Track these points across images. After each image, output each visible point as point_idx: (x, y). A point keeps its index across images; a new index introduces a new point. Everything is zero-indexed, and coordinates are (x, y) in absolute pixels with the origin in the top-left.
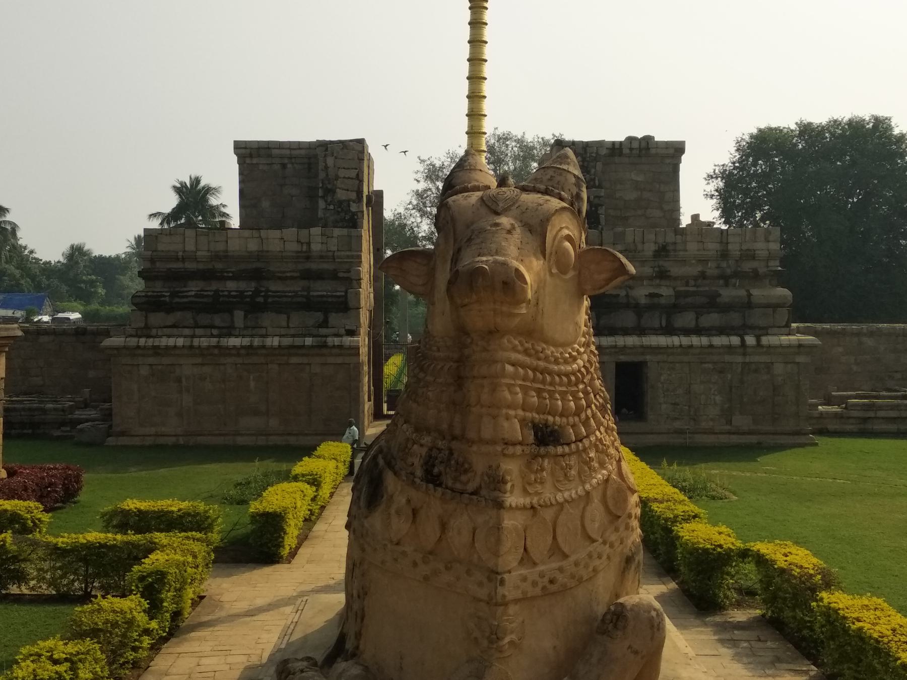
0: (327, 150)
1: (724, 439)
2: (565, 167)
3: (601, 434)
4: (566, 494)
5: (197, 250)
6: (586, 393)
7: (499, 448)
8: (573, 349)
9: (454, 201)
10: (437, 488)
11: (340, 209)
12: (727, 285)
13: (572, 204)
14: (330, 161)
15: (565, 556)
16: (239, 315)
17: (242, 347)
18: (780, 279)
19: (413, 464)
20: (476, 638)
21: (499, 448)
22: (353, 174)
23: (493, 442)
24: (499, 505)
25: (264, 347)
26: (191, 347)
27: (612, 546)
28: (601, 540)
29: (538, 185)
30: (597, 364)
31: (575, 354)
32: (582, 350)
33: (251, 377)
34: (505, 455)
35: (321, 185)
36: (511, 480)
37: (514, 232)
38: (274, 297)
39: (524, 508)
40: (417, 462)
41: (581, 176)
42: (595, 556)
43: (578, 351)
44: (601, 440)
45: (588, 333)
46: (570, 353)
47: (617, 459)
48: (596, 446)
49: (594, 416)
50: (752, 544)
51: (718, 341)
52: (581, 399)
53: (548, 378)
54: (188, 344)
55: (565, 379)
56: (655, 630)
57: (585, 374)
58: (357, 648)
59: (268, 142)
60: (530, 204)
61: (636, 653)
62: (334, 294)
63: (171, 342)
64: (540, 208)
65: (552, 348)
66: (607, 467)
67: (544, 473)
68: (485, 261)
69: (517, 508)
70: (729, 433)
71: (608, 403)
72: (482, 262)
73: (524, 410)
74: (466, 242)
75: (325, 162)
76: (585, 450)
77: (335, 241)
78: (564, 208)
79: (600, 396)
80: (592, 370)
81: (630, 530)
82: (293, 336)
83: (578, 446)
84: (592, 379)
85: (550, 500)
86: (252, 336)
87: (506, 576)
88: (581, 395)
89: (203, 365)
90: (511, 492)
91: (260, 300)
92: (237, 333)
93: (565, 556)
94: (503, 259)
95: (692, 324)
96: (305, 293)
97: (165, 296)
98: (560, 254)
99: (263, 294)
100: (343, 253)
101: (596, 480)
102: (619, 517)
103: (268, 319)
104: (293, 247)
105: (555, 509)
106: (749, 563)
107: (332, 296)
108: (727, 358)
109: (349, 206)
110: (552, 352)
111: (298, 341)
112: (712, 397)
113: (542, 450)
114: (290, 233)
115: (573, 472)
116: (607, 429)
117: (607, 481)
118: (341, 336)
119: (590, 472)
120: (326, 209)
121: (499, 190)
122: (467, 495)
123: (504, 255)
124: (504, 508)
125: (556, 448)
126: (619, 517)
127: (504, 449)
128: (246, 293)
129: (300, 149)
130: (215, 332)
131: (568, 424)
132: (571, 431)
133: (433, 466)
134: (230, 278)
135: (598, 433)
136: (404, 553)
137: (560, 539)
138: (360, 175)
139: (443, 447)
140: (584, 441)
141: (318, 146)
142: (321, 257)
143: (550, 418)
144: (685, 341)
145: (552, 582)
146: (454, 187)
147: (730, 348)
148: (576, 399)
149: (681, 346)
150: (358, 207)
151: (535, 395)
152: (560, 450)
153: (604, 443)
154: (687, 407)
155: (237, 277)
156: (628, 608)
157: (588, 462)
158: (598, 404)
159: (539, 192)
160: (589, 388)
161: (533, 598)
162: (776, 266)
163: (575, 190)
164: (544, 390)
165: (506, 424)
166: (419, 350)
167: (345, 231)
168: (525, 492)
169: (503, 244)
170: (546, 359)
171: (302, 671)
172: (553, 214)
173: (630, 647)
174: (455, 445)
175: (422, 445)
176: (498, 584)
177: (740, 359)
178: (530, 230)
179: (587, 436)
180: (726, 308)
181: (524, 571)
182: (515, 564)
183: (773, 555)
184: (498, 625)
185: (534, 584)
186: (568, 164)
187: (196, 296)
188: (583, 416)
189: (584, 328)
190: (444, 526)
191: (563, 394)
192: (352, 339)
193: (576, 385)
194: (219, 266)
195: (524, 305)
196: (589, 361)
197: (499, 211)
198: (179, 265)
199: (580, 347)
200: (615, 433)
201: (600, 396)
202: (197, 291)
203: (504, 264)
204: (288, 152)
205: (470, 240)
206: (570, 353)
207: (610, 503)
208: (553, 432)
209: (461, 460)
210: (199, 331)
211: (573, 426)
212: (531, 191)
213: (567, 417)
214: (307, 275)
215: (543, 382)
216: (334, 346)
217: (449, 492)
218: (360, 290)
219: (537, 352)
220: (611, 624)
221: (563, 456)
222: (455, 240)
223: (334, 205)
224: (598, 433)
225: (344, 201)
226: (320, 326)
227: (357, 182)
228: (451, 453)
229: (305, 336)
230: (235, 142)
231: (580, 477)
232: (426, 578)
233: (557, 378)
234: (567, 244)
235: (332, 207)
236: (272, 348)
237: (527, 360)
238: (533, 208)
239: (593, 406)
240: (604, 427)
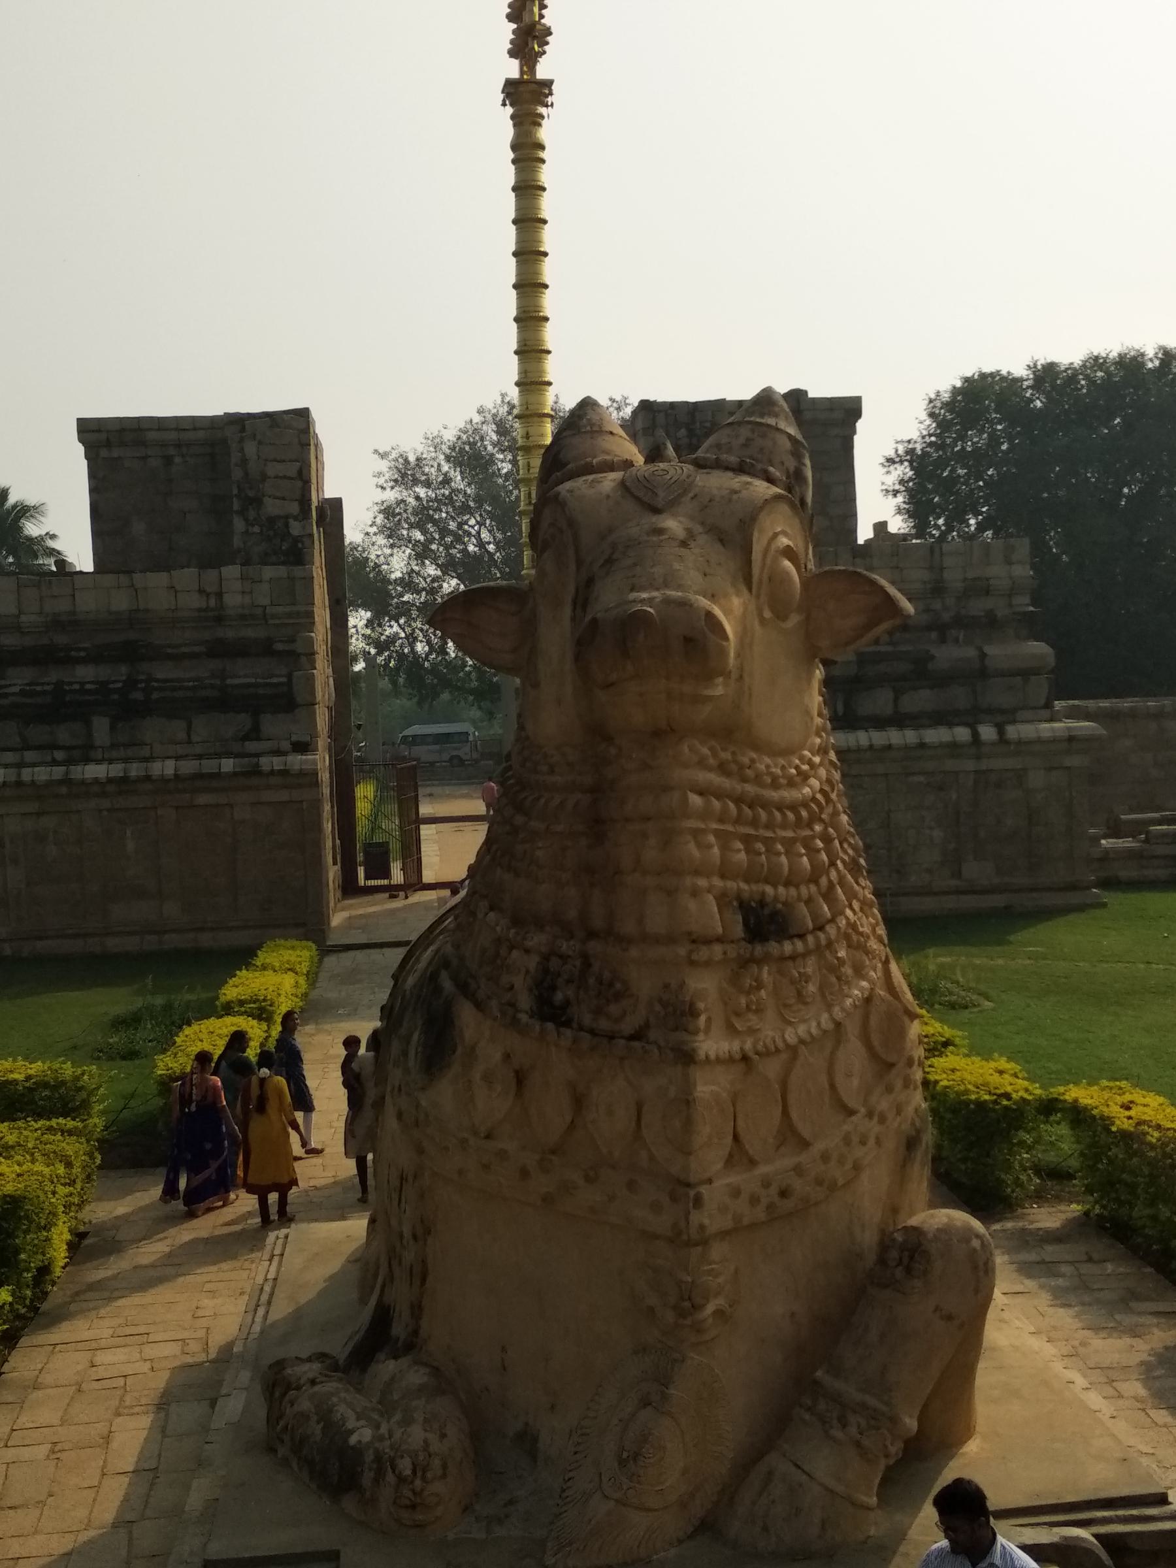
0: (243, 429)
1: (950, 903)
2: (771, 421)
3: (855, 913)
4: (802, 1030)
5: (20, 613)
6: (827, 840)
7: (682, 951)
8: (802, 758)
9: (571, 491)
10: (562, 1029)
11: (271, 533)
12: (943, 640)
13: (789, 489)
14: (250, 448)
15: (805, 1144)
16: (101, 727)
17: (110, 780)
18: (1031, 626)
19: (512, 988)
20: (651, 1310)
21: (682, 951)
22: (292, 470)
23: (670, 939)
24: (687, 1058)
25: (148, 778)
26: (19, 784)
27: (882, 1119)
28: (863, 1110)
29: (724, 457)
30: (840, 785)
31: (805, 767)
32: (817, 759)
33: (128, 833)
34: (692, 963)
35: (235, 491)
36: (706, 1010)
37: (692, 544)
39: (731, 1060)
40: (519, 981)
41: (799, 437)
42: (855, 1139)
43: (810, 763)
44: (853, 926)
45: (824, 729)
46: (797, 768)
47: (883, 959)
48: (847, 937)
49: (842, 881)
50: (1061, 1089)
51: (936, 735)
52: (818, 851)
53: (763, 815)
54: (13, 779)
55: (791, 816)
56: (981, 1274)
57: (823, 802)
58: (416, 1332)
59: (138, 419)
60: (715, 492)
61: (949, 1318)
62: (268, 681)
64: (735, 497)
65: (768, 760)
66: (867, 974)
67: (763, 993)
68: (646, 600)
69: (718, 1060)
70: (959, 892)
71: (860, 856)
72: (642, 601)
73: (723, 877)
74: (602, 566)
75: (242, 450)
76: (830, 944)
78: (778, 497)
79: (850, 844)
80: (834, 796)
81: (912, 1087)
82: (200, 757)
83: (817, 939)
84: (835, 814)
85: (774, 1041)
86: (126, 760)
87: (704, 1189)
88: (820, 844)
89: (39, 814)
90: (707, 1030)
91: (138, 696)
92: (100, 757)
93: (805, 1144)
94: (680, 594)
95: (889, 710)
98: (777, 579)
99: (143, 685)
100: (280, 609)
101: (851, 1000)
102: (892, 1065)
104: (194, 601)
105: (784, 1056)
106: (1058, 1123)
108: (950, 765)
109: (287, 525)
110: (768, 767)
111: (209, 766)
113: (759, 949)
114: (186, 577)
115: (812, 988)
116: (864, 903)
117: (868, 1000)
118: (284, 754)
119: (840, 986)
120: (247, 532)
121: (651, 467)
122: (622, 1042)
123: (679, 587)
124: (695, 1063)
125: (782, 946)
126: (892, 1065)
127: (691, 952)
128: (111, 686)
129: (195, 429)
130: (59, 755)
131: (799, 899)
132: (805, 909)
133: (553, 988)
134: (84, 661)
135: (848, 912)
136: (502, 1155)
137: (794, 1115)
138: (304, 472)
139: (570, 953)
140: (828, 928)
142: (243, 617)
143: (769, 890)
144: (879, 738)
145: (784, 1194)
146: (566, 464)
147: (954, 748)
148: (812, 851)
149: (871, 747)
150: (304, 528)
151: (741, 846)
152: (788, 947)
153: (861, 929)
155: (96, 657)
156: (930, 1236)
157: (835, 969)
158: (846, 858)
159: (727, 468)
160: (831, 830)
161: (753, 1226)
162: (1023, 602)
163: (791, 464)
164: (757, 838)
165: (692, 905)
166: (510, 773)
167: (282, 571)
168: (731, 1030)
169: (676, 566)
170: (758, 780)
171: (313, 1382)
172: (761, 508)
173: (937, 1309)
174: (594, 947)
175: (527, 951)
176: (691, 1204)
177: (970, 765)
178: (721, 541)
179: (832, 920)
181: (734, 1179)
182: (719, 1166)
183: (1105, 1109)
184: (693, 1282)
185: (754, 1200)
186: (776, 416)
187: (23, 693)
188: (824, 881)
189: (818, 721)
190: (579, 1102)
191: (789, 843)
192: (304, 757)
193: (810, 826)
194: (61, 639)
195: (721, 679)
196: (829, 781)
197: (660, 506)
199: (813, 755)
200: (876, 911)
201: (850, 844)
202: (27, 684)
203: (684, 604)
204: (173, 436)
205: (609, 561)
206: (797, 768)
207: (876, 1041)
208: (775, 914)
209: (607, 975)
210: (30, 756)
211: (809, 901)
212: (712, 468)
213: (797, 887)
214: (219, 650)
215: (754, 823)
216: (272, 773)
217: (587, 1036)
218: (315, 671)
219: (741, 767)
220: (900, 1268)
221: (793, 958)
222: (579, 563)
224: (848, 912)
225: (279, 517)
226: (246, 738)
227: (299, 484)
228: (587, 963)
229: (219, 756)
231: (823, 996)
232: (547, 1199)
233: (777, 814)
234: (787, 564)
235: (256, 529)
236: (164, 780)
237: (725, 783)
238: (722, 497)
239: (839, 862)
240: (859, 900)
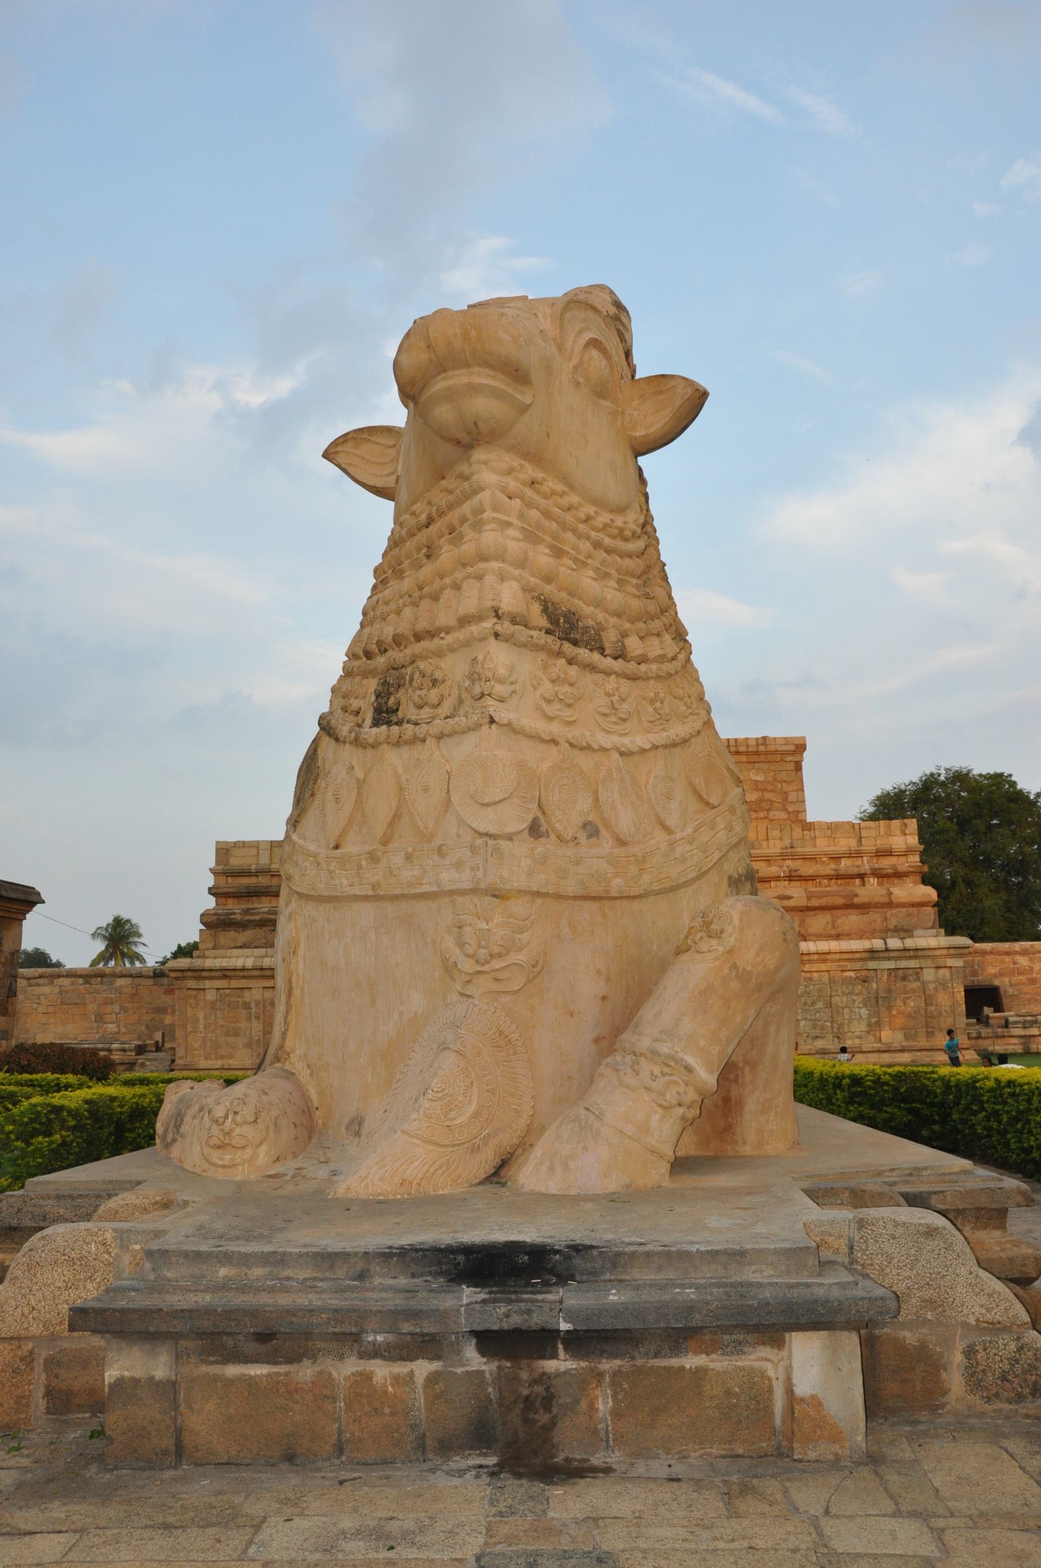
63: (239, 963)
70: (879, 1051)
97: (234, 913)
112: (857, 1010)
144: (823, 946)
147: (873, 954)
154: (829, 1024)
180: (864, 908)
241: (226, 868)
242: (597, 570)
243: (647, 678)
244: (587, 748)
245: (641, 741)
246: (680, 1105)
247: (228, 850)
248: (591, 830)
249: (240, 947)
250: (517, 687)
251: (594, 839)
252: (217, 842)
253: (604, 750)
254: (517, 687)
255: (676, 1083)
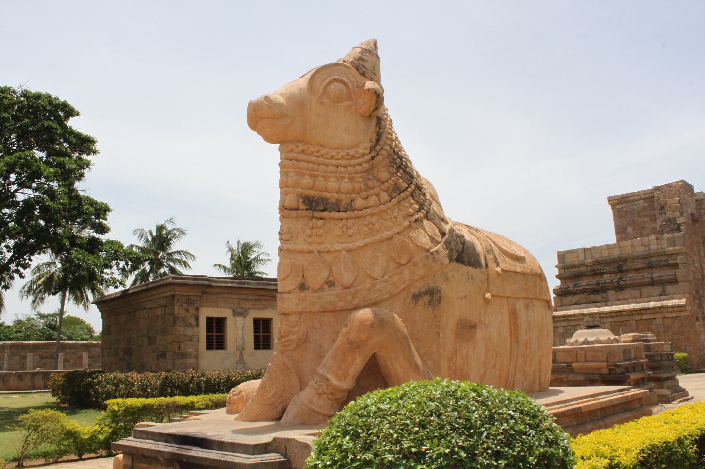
5: (585, 259)
33: (621, 329)
38: (631, 280)
77: (665, 242)
96: (649, 276)
97: (569, 287)
103: (627, 293)
107: (667, 276)
109: (675, 220)
129: (645, 194)
141: (655, 190)
194: (597, 267)
198: (577, 269)
223: (666, 222)
225: (672, 218)
226: (660, 295)
230: (608, 198)
241: (563, 264)
242: (336, 177)
243: (365, 217)
244: (328, 252)
245: (359, 243)
246: (325, 394)
247: (563, 255)
248: (331, 284)
249: (574, 304)
250: (294, 234)
251: (332, 288)
252: (558, 252)
253: (340, 251)
254: (294, 234)
255: (322, 385)
